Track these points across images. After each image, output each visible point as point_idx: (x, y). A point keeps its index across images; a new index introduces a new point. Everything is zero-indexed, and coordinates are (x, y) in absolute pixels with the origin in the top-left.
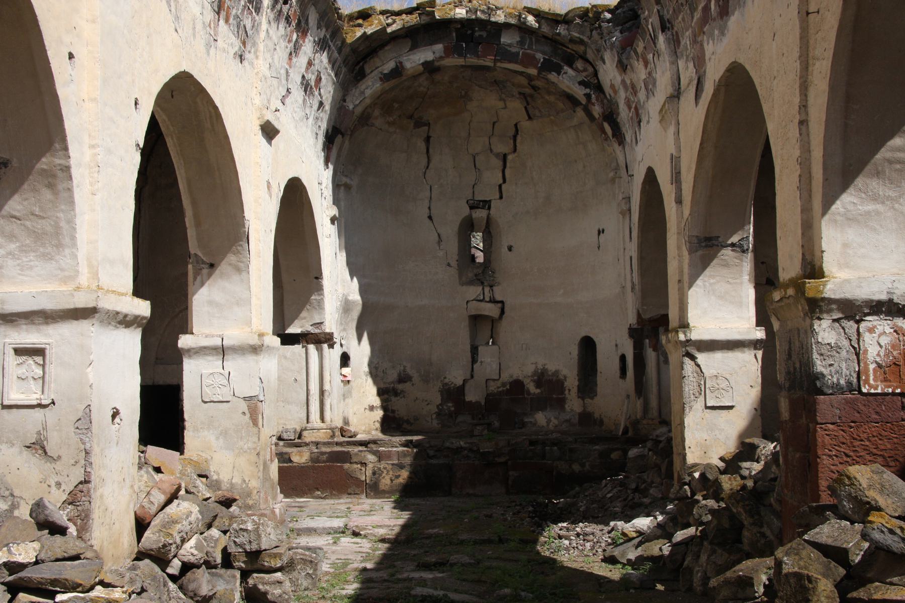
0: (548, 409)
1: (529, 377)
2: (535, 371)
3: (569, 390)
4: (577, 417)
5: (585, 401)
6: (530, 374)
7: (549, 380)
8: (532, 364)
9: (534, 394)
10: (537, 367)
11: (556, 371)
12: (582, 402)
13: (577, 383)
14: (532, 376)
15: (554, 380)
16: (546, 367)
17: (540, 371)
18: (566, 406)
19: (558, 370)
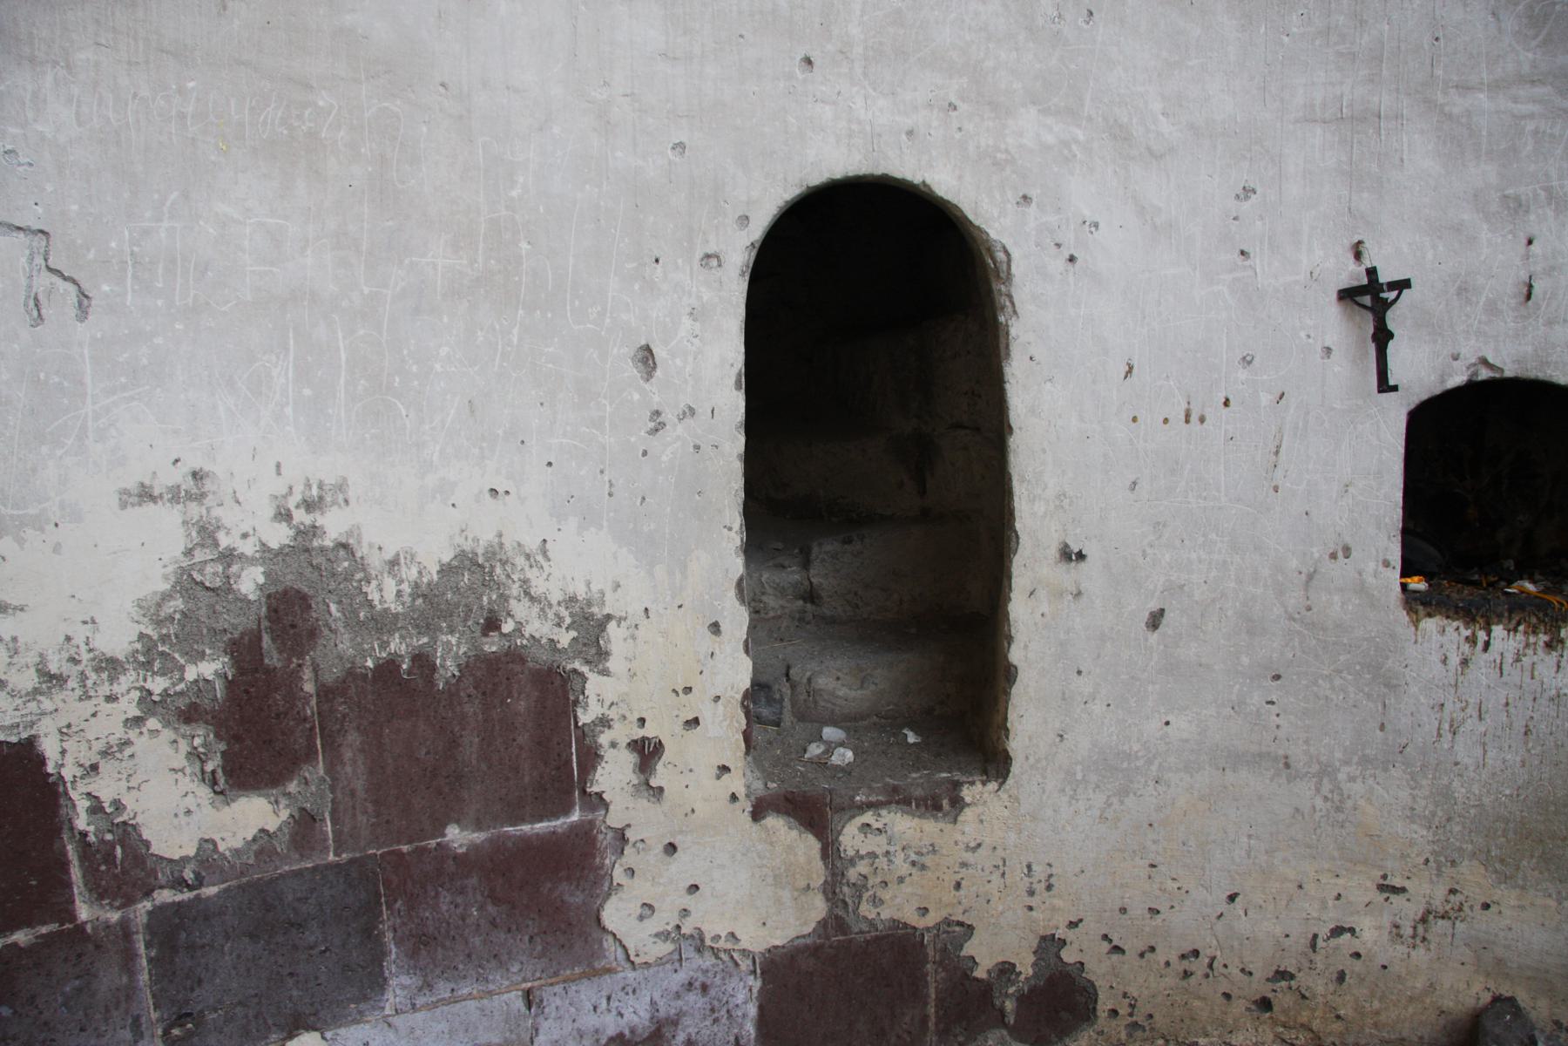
0: (399, 985)
1: (111, 666)
2: (187, 583)
3: (647, 753)
4: (744, 995)
5: (851, 837)
6: (119, 638)
7: (389, 667)
8: (146, 495)
9: (207, 858)
10: (207, 533)
11: (465, 562)
12: (811, 844)
13: (738, 673)
14: (149, 656)
15: (448, 667)
16: (333, 525)
17: (250, 581)
18: (616, 914)
19: (495, 553)
